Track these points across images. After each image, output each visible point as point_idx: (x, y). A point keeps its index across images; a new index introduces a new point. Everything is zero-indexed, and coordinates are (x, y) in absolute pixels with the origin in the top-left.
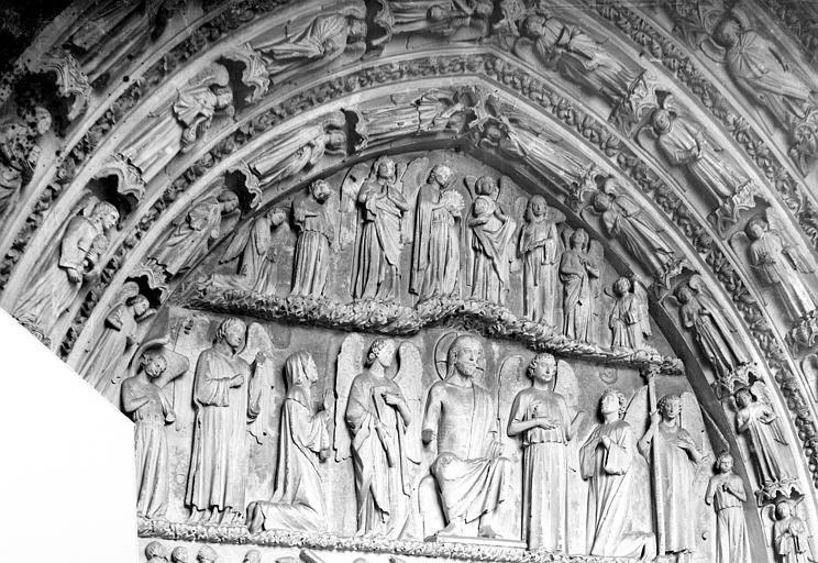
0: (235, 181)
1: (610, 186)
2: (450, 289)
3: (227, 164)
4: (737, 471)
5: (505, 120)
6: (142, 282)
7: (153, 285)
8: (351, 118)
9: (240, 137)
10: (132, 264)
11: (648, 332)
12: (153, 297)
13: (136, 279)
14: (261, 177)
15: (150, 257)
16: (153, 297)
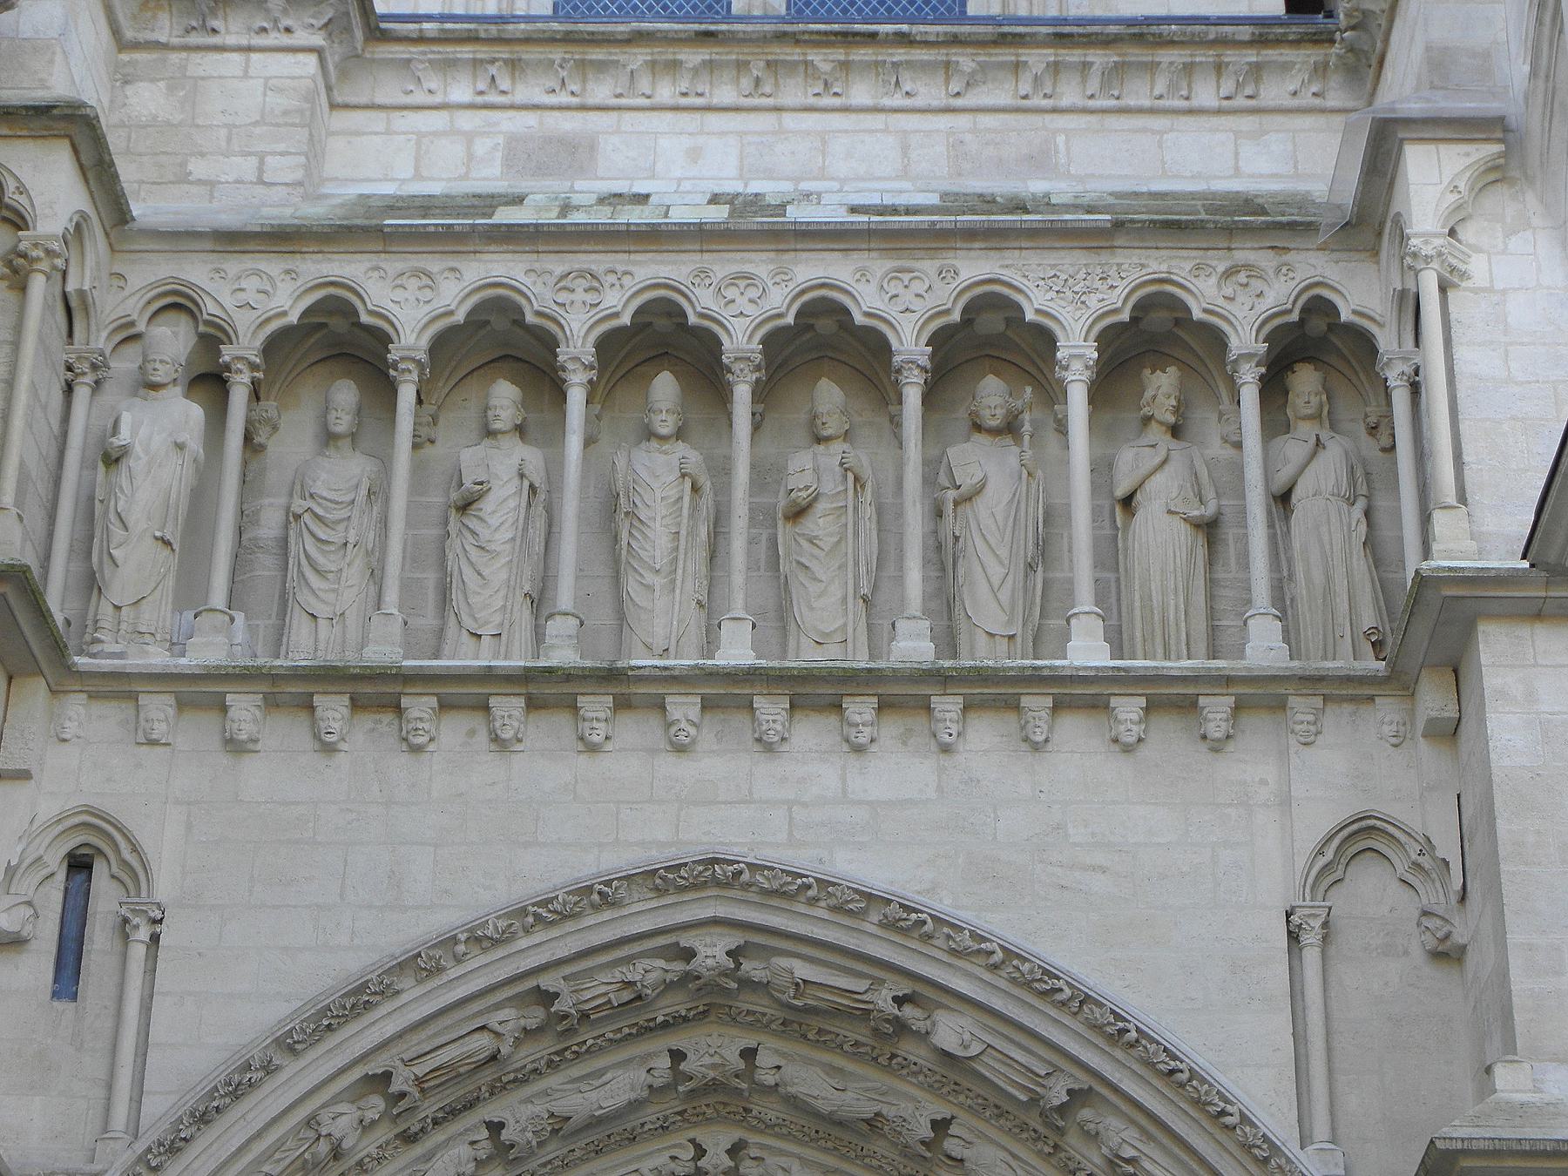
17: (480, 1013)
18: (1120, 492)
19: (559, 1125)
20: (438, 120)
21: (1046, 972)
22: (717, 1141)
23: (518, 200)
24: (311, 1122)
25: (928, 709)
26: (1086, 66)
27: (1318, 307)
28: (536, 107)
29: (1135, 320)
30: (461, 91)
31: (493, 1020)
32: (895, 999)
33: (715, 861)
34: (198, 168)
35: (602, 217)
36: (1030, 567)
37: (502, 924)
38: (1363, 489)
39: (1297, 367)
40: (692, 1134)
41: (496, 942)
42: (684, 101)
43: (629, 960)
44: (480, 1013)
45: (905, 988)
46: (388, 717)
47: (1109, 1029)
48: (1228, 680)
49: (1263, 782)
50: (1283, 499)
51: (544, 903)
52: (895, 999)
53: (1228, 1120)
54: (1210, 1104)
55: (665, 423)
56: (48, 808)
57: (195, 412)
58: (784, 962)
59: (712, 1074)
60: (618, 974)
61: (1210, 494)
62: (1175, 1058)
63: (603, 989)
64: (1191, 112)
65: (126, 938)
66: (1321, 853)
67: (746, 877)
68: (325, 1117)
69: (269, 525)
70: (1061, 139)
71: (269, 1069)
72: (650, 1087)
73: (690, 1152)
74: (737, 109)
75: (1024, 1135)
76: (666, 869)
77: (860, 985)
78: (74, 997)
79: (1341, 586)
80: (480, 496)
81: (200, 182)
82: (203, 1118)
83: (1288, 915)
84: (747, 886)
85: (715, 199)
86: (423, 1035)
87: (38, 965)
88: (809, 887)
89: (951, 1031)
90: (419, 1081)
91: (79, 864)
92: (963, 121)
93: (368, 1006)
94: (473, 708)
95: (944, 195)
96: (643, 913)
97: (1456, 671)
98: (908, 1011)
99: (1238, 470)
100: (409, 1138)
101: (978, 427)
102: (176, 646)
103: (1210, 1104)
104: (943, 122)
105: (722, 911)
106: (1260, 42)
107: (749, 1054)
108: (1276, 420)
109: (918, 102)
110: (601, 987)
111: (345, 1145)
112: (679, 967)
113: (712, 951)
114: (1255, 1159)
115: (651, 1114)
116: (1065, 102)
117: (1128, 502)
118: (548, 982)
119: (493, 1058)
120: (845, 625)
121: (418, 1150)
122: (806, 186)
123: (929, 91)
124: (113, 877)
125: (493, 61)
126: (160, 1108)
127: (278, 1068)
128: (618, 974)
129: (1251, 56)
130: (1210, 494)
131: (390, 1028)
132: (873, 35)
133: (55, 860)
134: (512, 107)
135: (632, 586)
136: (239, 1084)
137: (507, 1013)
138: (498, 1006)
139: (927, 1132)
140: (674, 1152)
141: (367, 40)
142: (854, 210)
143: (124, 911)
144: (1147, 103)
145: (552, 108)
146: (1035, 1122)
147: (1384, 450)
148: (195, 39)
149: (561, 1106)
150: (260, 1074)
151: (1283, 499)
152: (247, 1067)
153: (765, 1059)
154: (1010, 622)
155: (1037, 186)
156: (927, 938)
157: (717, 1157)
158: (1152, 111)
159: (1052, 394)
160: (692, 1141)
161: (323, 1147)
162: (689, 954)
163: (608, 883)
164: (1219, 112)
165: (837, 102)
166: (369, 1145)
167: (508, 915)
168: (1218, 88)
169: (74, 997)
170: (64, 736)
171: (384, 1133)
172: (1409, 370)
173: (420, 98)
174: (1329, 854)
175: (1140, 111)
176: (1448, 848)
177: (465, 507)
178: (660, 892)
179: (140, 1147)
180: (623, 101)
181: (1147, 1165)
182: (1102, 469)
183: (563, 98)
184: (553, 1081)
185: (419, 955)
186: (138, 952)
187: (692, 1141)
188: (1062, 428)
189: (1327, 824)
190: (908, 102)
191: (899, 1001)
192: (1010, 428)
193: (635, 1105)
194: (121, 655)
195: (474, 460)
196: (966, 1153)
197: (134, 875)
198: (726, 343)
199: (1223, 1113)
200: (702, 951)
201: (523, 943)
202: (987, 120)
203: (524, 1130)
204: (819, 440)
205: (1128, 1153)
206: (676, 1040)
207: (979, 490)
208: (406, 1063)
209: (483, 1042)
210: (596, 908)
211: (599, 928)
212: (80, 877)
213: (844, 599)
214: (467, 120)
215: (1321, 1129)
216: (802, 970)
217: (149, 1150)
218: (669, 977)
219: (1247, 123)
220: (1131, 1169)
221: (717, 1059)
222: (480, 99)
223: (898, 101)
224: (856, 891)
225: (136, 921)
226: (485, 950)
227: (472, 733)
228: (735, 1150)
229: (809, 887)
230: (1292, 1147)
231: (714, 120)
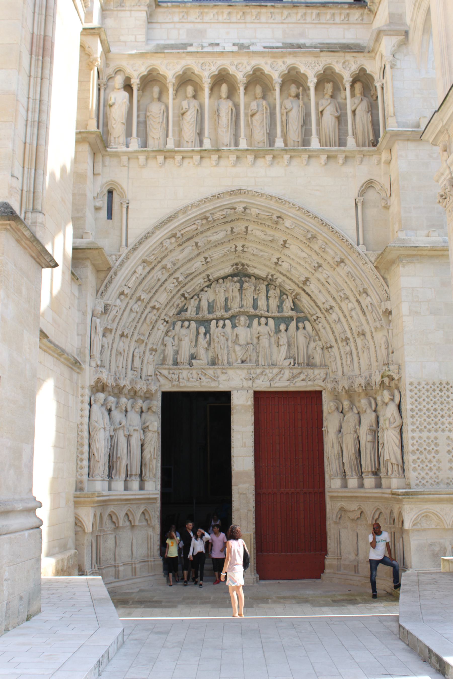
0: (183, 295)
1: (275, 277)
2: (235, 308)
3: (181, 292)
4: (320, 340)
5: (246, 267)
6: (164, 320)
7: (166, 320)
8: (208, 276)
9: (183, 287)
10: (163, 316)
11: (293, 307)
12: (167, 322)
14: (188, 293)
15: (166, 315)
16: (167, 322)
17: (194, 221)
18: (320, 109)
20: (171, 26)
21: (307, 212)
23: (191, 45)
24: (161, 243)
25: (283, 157)
26: (312, 13)
27: (362, 70)
28: (193, 22)
29: (324, 72)
30: (176, 19)
31: (196, 222)
33: (240, 190)
34: (122, 39)
35: (209, 49)
36: (302, 126)
37: (198, 203)
38: (370, 109)
39: (357, 82)
42: (225, 21)
43: (223, 210)
44: (194, 221)
46: (172, 160)
48: (344, 152)
49: (351, 172)
50: (354, 112)
51: (206, 199)
53: (344, 241)
55: (224, 95)
56: (105, 181)
57: (126, 94)
60: (221, 213)
61: (339, 110)
62: (333, 228)
64: (334, 24)
65: (122, 207)
66: (362, 187)
67: (247, 193)
68: (164, 242)
69: (142, 119)
70: (306, 30)
73: (234, 247)
74: (236, 23)
76: (231, 191)
78: (111, 219)
79: (366, 130)
80: (187, 111)
81: (123, 42)
82: (140, 243)
83: (355, 200)
85: (234, 45)
86: (183, 225)
87: (104, 213)
88: (259, 195)
90: (182, 235)
91: (110, 192)
92: (285, 26)
93: (172, 220)
94: (190, 158)
95: (283, 43)
96: (227, 201)
97: (390, 150)
98: (279, 219)
99: (345, 105)
100: (180, 245)
101: (290, 96)
102: (127, 146)
104: (281, 26)
105: (242, 200)
106: (350, 8)
107: (246, 228)
108: (353, 95)
109: (276, 21)
110: (218, 215)
111: (168, 247)
115: (226, 240)
116: (307, 22)
117: (322, 112)
118: (208, 215)
119: (196, 229)
120: (264, 140)
121: (181, 248)
122: (253, 41)
123: (278, 18)
124: (118, 194)
125: (183, 12)
126: (132, 241)
129: (348, 11)
130: (339, 110)
131: (177, 224)
132: (266, 6)
133: (106, 192)
134: (187, 22)
135: (220, 130)
136: (147, 237)
137: (199, 221)
138: (197, 220)
139: (282, 243)
141: (156, 7)
142: (265, 47)
143: (121, 201)
144: (325, 22)
145: (196, 23)
147: (374, 100)
148: (119, 8)
149: (209, 239)
151: (354, 112)
152: (149, 233)
153: (249, 229)
154: (298, 138)
155: (302, 41)
157: (239, 248)
158: (326, 23)
159: (306, 89)
160: (235, 245)
161: (164, 248)
163: (219, 194)
164: (340, 24)
165: (258, 21)
166: (172, 247)
167: (199, 201)
168: (340, 18)
169: (111, 219)
170: (106, 165)
171: (176, 245)
172: (381, 84)
173: (167, 20)
174: (364, 187)
175: (323, 23)
176: (387, 186)
177: (183, 114)
179: (129, 249)
180: (212, 21)
182: (317, 104)
183: (199, 20)
184: (208, 233)
186: (124, 210)
187: (235, 245)
188: (308, 96)
189: (363, 181)
190: (273, 21)
192: (297, 96)
193: (224, 238)
194: (116, 148)
195: (185, 104)
197: (122, 195)
198: (238, 78)
199: (342, 239)
200: (238, 208)
202: (291, 25)
204: (256, 98)
205: (323, 247)
206: (231, 225)
207: (291, 110)
208: (180, 231)
209: (194, 227)
212: (110, 194)
213: (264, 134)
214: (178, 26)
215: (361, 241)
217: (131, 250)
219: (346, 26)
222: (181, 21)
223: (271, 21)
227: (189, 163)
228: (243, 246)
229: (259, 195)
230: (356, 246)
231: (231, 25)
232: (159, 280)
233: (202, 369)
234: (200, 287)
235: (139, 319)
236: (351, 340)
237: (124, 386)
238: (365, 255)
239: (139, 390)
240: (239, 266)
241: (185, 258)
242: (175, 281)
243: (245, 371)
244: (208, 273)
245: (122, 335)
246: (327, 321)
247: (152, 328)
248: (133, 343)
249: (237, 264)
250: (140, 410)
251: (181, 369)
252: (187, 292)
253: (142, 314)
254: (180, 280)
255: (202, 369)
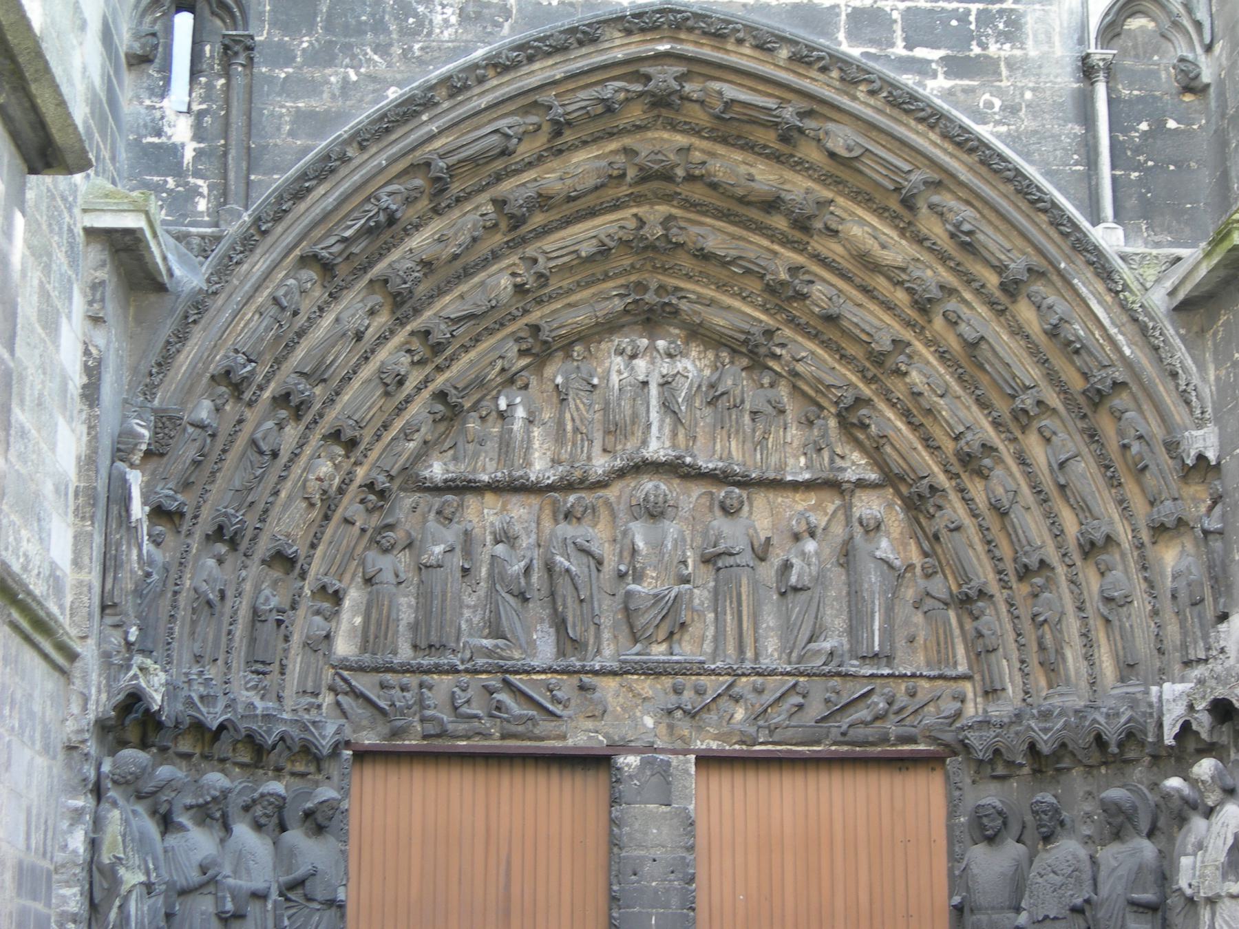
0: (441, 396)
8: (535, 329)
13: (365, 486)
19: (543, 201)
22: (656, 213)
32: (798, 114)
40: (635, 210)
41: (506, 69)
45: (805, 105)
47: (958, 139)
52: (798, 114)
54: (1030, 194)
58: (716, 85)
59: (656, 167)
60: (593, 93)
63: (583, 104)
71: (344, 159)
72: (610, 176)
75: (886, 214)
77: (771, 103)
84: (691, 30)
88: (739, 31)
89: (841, 138)
96: (619, 48)
98: (810, 124)
103: (1030, 194)
111: (399, 215)
112: (638, 87)
113: (664, 77)
114: (1062, 233)
118: (548, 97)
127: (350, 159)
128: (593, 93)
140: (622, 223)
146: (894, 204)
150: (338, 163)
156: (824, 70)
162: (648, 78)
163: (590, 25)
178: (629, 32)
181: (981, 237)
185: (451, 77)
191: (802, 115)
196: (840, 228)
201: (526, 69)
203: (521, 206)
210: (581, 43)
211: (583, 59)
216: (731, 92)
218: (630, 95)
220: (968, 239)
221: (660, 157)
224: (773, 35)
225: (237, 48)
226: (499, 74)
229: (739, 31)
232: (359, 336)
233: (507, 671)
234: (503, 370)
235: (282, 479)
236: (1061, 570)
237: (222, 727)
238: (1120, 261)
239: (274, 747)
240: (647, 297)
241: (456, 257)
242: (416, 344)
243: (667, 682)
244: (534, 317)
245: (218, 534)
246: (967, 501)
247: (327, 518)
248: (255, 568)
249: (641, 287)
250: (275, 820)
251: (428, 672)
252: (456, 388)
253: (291, 460)
254: (433, 339)
255: (507, 671)
